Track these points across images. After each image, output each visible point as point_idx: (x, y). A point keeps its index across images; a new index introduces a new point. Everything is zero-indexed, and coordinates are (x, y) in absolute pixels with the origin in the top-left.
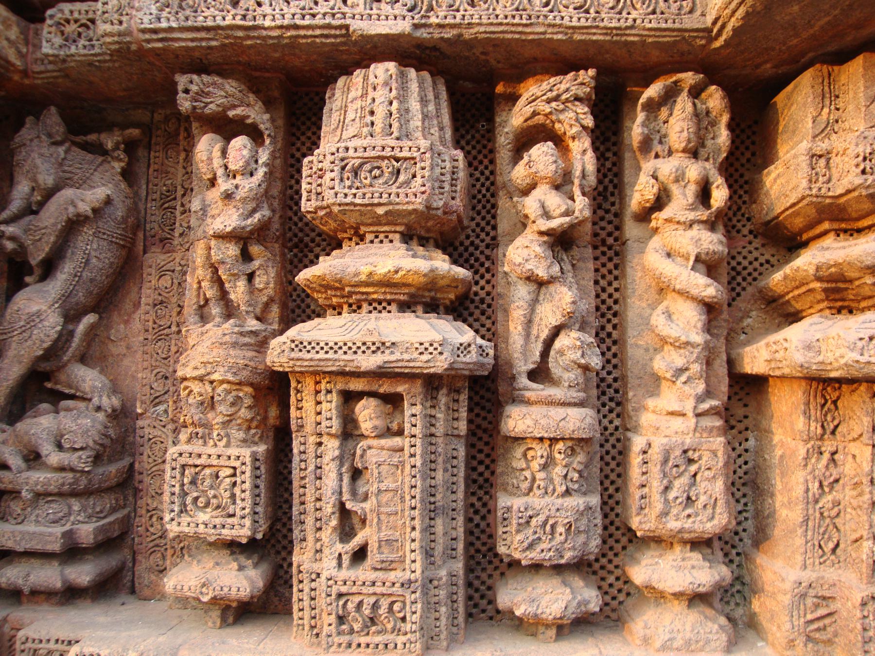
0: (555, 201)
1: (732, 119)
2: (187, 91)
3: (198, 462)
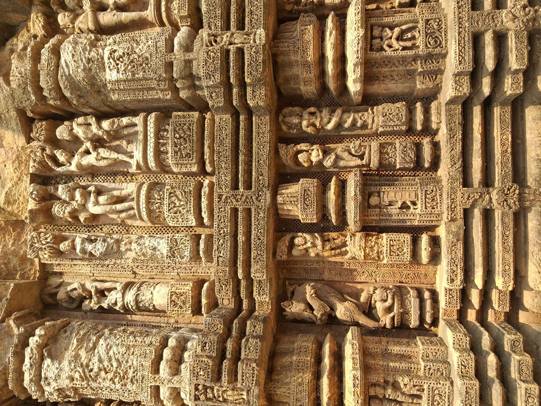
0: (314, 153)
1: (290, 106)
2: (281, 257)
3: (389, 251)
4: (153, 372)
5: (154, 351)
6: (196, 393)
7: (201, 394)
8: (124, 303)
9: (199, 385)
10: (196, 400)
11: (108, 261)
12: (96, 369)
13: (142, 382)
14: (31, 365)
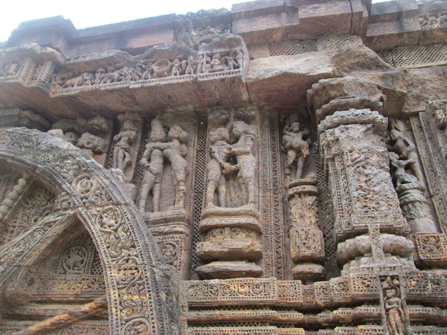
4: (382, 227)
5: (400, 226)
6: (389, 277)
7: (388, 282)
8: (408, 189)
9: (398, 279)
10: (380, 277)
11: (439, 171)
12: (367, 171)
13: (369, 217)
14: (357, 115)
